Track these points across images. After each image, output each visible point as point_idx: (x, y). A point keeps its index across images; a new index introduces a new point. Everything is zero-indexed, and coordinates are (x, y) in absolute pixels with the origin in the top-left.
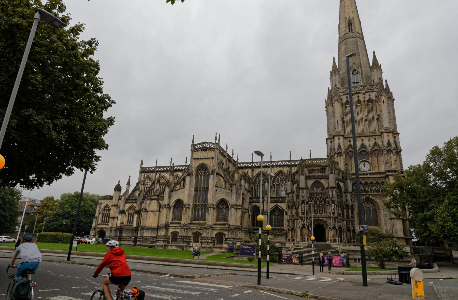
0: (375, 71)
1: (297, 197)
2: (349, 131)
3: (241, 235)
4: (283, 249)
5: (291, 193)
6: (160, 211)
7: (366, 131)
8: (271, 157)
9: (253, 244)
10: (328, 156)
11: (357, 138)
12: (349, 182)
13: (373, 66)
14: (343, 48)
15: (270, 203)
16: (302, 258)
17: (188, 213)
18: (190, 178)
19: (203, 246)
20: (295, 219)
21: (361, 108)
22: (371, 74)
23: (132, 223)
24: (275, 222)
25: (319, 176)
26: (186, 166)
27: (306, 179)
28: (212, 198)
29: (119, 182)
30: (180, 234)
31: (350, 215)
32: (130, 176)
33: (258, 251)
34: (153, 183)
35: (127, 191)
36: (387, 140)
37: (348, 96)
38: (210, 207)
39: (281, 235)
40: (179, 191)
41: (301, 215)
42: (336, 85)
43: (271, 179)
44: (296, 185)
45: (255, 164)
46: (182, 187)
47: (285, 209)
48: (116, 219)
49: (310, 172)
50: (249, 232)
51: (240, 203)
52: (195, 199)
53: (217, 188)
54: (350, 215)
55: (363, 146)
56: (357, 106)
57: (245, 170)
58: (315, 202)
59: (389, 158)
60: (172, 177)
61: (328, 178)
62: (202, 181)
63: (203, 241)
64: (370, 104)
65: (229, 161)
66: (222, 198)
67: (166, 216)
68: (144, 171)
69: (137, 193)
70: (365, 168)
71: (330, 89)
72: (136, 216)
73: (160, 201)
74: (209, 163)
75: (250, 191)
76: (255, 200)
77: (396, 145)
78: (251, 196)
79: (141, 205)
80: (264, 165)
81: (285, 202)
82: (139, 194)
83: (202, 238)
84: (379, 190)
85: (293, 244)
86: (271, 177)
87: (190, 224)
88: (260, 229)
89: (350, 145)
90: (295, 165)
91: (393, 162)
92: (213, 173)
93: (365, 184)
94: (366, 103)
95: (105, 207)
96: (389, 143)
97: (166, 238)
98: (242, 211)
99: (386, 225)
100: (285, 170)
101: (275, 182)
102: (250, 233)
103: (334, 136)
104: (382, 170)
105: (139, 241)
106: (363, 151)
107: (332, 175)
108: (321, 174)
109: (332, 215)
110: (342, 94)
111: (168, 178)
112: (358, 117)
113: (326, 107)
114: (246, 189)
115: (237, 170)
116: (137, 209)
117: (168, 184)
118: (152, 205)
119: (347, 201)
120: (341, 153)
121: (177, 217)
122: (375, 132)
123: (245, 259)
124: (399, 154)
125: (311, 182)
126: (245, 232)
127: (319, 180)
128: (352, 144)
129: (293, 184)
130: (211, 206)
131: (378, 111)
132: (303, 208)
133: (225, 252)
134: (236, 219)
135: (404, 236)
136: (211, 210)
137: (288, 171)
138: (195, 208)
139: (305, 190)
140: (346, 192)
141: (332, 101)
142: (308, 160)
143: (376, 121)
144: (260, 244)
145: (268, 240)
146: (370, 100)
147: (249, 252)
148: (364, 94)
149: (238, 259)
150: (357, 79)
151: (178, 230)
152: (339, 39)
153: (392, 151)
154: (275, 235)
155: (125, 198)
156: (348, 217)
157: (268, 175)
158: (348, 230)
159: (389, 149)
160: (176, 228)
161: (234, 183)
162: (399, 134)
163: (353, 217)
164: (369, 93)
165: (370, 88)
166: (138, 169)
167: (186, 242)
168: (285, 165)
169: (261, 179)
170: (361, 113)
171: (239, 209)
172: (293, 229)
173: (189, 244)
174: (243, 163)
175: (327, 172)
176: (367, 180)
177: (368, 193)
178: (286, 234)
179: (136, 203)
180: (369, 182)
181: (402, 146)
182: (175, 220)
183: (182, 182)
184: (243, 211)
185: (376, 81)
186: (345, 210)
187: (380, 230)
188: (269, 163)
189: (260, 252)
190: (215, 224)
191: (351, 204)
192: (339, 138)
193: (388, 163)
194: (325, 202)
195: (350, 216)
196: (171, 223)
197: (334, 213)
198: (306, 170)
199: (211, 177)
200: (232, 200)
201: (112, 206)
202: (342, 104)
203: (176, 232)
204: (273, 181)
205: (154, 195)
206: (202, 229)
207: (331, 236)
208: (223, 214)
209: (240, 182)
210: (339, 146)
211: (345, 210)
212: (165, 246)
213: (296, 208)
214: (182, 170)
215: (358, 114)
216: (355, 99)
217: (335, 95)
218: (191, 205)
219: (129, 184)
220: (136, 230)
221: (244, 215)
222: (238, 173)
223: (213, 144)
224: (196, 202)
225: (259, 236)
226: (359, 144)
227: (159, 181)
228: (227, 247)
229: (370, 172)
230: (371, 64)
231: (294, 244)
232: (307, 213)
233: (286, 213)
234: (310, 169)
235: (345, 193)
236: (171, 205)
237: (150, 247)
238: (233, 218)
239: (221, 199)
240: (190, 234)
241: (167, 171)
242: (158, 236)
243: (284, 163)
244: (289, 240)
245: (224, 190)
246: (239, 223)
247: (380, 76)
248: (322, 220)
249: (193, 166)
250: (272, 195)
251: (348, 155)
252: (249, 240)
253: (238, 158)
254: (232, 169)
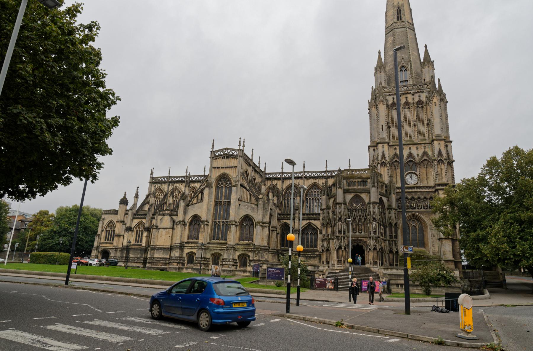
0: (427, 67)
1: (334, 213)
2: (395, 139)
3: (268, 257)
4: (316, 272)
5: (326, 209)
6: (173, 229)
7: (414, 138)
8: (304, 167)
9: (281, 267)
10: (370, 166)
11: (403, 146)
12: (394, 197)
13: (424, 63)
14: (390, 39)
15: (302, 220)
16: (337, 283)
17: (206, 230)
18: (210, 190)
19: (223, 268)
20: (330, 239)
21: (409, 111)
22: (421, 71)
23: (141, 242)
24: (308, 242)
25: (359, 189)
26: (205, 176)
27: (344, 193)
28: (235, 213)
29: (125, 194)
30: (197, 256)
31: (394, 234)
32: (138, 187)
33: (287, 275)
34: (166, 196)
35: (135, 205)
36: (438, 149)
37: (395, 97)
38: (233, 225)
39: (314, 257)
40: (196, 205)
41: (337, 234)
42: (381, 84)
43: (304, 192)
44: (332, 200)
45: (285, 175)
46: (199, 201)
47: (319, 228)
48: (122, 237)
49: (349, 185)
50: (277, 253)
51: (267, 219)
52: (215, 215)
53: (241, 203)
54: (394, 234)
55: (410, 155)
56: (405, 108)
57: (273, 182)
58: (354, 219)
59: (439, 169)
60: (187, 188)
61: (370, 192)
62: (223, 194)
63: (224, 263)
64: (420, 106)
65: (255, 171)
66: (246, 214)
67: (181, 234)
68: (154, 181)
69: (146, 208)
70: (412, 180)
71: (374, 88)
72: (145, 234)
73: (174, 217)
74: (230, 172)
75: (279, 206)
76: (284, 216)
77: (448, 154)
78: (280, 212)
79: (151, 221)
80: (296, 176)
81: (319, 220)
82: (149, 209)
83: (223, 259)
84: (427, 206)
85: (327, 267)
86: (304, 189)
87: (208, 243)
88: (290, 249)
89: (396, 154)
90: (332, 177)
91: (444, 174)
92: (236, 185)
93: (411, 199)
94: (415, 105)
95: (109, 224)
96: (440, 153)
97: (180, 260)
98: (269, 229)
99: (433, 246)
100: (320, 182)
101: (309, 195)
102: (278, 254)
103: (378, 144)
104: (432, 183)
105: (149, 263)
106: (411, 161)
108: (362, 187)
109: (372, 235)
110: (388, 94)
111: (183, 190)
112: (406, 122)
113: (369, 109)
114: (274, 204)
115: (265, 182)
116: (147, 225)
117: (183, 196)
118: (164, 221)
119: (390, 218)
120: (385, 164)
121: (194, 235)
122: (424, 140)
123: (273, 284)
124: (450, 165)
125: (349, 197)
126: (273, 253)
127: (359, 194)
128: (398, 153)
129: (329, 199)
130: (234, 223)
131: (429, 115)
132: (340, 226)
133: (249, 276)
134: (263, 239)
135: (453, 259)
136: (233, 228)
137: (323, 184)
138: (215, 225)
139: (343, 206)
140: (390, 208)
141: (376, 102)
142: (347, 170)
143: (426, 126)
144: (290, 267)
145: (299, 262)
146: (420, 102)
147: (277, 276)
148: (413, 95)
149: (265, 284)
150: (406, 77)
151: (195, 251)
152: (386, 29)
153: (443, 162)
154: (307, 257)
155: (132, 213)
156: (391, 236)
157: (300, 188)
158: (391, 251)
159: (440, 159)
160: (192, 248)
161: (260, 197)
162: (451, 142)
163: (396, 237)
164: (419, 94)
165: (420, 88)
166: (148, 180)
167: (204, 264)
168: (321, 177)
169: (293, 192)
170: (409, 117)
171: (266, 226)
172: (328, 250)
173: (208, 266)
174: (271, 174)
175: (368, 184)
176: (413, 194)
177: (415, 210)
178: (320, 256)
179: (145, 218)
180: (416, 197)
181: (455, 155)
182: (190, 239)
183: (200, 195)
184: (271, 229)
185: (428, 79)
186: (388, 229)
187: (427, 252)
188: (302, 174)
189: (289, 276)
190: (238, 244)
191: (395, 222)
192: (383, 146)
193: (438, 175)
194: (365, 219)
195: (393, 236)
196: (186, 243)
197: (375, 232)
198: (345, 182)
199: (234, 189)
200: (258, 216)
201: (117, 222)
202: (387, 106)
203: (192, 252)
204: (306, 195)
205: (166, 210)
206: (222, 250)
207: (371, 259)
208: (247, 233)
209: (268, 196)
210: (383, 156)
211: (388, 229)
212: (179, 268)
213: (331, 227)
214: (199, 181)
215: (406, 118)
216: (403, 100)
217: (380, 95)
218: (210, 221)
219: (137, 196)
220: (146, 250)
221: (272, 234)
222: (265, 185)
223: (236, 150)
224: (216, 219)
225: (288, 257)
226: (406, 153)
227: (172, 194)
228: (252, 270)
229: (417, 185)
230: (422, 60)
231: (329, 267)
232: (344, 231)
233: (321, 232)
234: (349, 181)
235: (388, 209)
236: (186, 221)
237: (162, 270)
238: (259, 237)
239: (245, 215)
240: (208, 256)
241: (182, 182)
242: (172, 257)
243: (319, 174)
244: (323, 263)
245: (248, 204)
246: (265, 243)
247: (431, 74)
248: (361, 240)
249: (213, 177)
250: (304, 210)
251: (393, 165)
252: (277, 262)
253: (265, 168)
254: (258, 180)
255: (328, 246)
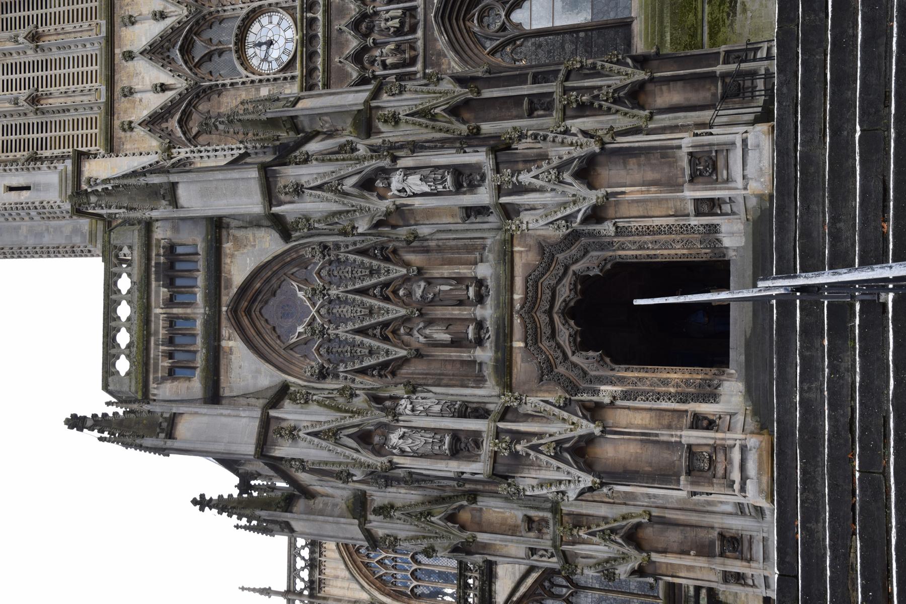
41: (478, 468)
55: (157, 51)
61: (217, 227)
106: (186, 50)
107: (184, 194)
109: (483, 196)
119: (425, 113)
127: (226, 299)
177: (420, 10)
194: (389, 255)
197: (465, 179)
198: (165, 391)
248: (533, 284)
255: (607, 535)
